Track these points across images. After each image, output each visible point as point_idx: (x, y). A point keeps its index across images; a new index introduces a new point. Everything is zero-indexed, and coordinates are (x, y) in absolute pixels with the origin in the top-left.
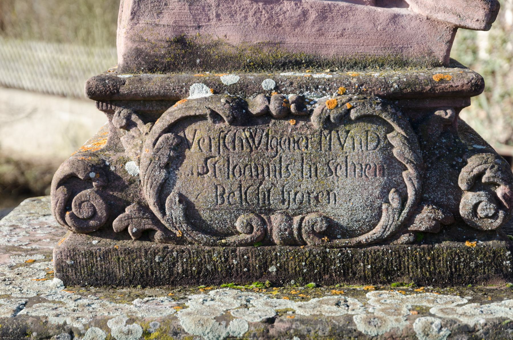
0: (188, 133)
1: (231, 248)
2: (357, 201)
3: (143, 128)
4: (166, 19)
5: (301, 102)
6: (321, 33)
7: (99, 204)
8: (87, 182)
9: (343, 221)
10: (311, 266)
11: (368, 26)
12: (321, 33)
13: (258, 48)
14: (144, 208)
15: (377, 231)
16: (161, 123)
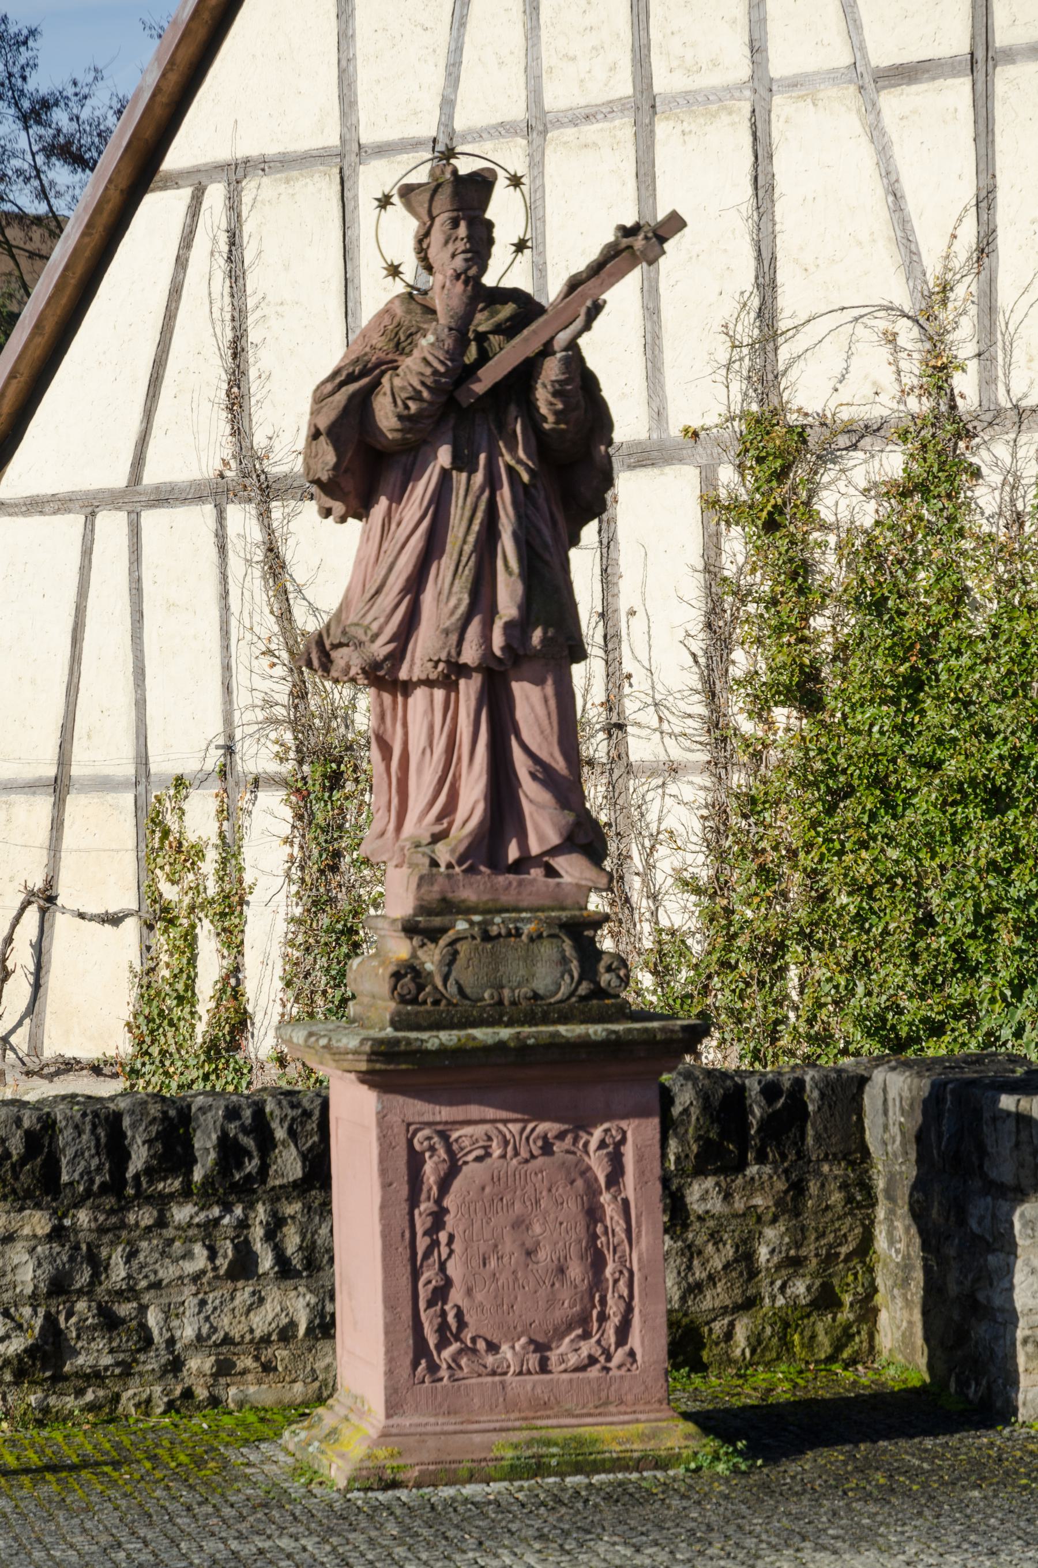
0: (458, 946)
1: (483, 1008)
2: (549, 980)
3: (432, 946)
4: (436, 888)
5: (517, 929)
6: (519, 893)
7: (412, 986)
8: (405, 975)
9: (541, 992)
10: (525, 1016)
11: (544, 889)
12: (519, 893)
13: (486, 902)
14: (436, 988)
15: (559, 996)
16: (442, 942)
